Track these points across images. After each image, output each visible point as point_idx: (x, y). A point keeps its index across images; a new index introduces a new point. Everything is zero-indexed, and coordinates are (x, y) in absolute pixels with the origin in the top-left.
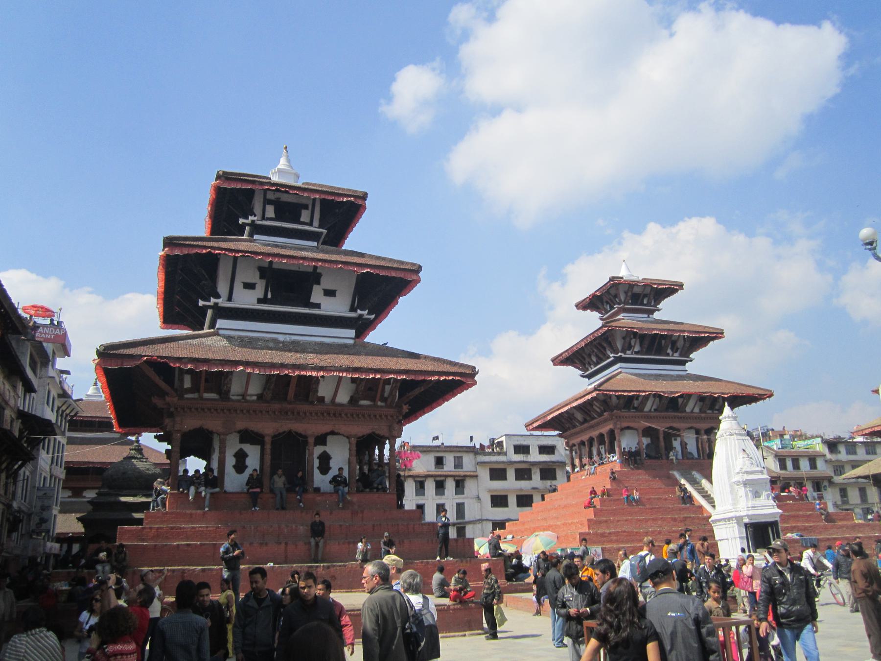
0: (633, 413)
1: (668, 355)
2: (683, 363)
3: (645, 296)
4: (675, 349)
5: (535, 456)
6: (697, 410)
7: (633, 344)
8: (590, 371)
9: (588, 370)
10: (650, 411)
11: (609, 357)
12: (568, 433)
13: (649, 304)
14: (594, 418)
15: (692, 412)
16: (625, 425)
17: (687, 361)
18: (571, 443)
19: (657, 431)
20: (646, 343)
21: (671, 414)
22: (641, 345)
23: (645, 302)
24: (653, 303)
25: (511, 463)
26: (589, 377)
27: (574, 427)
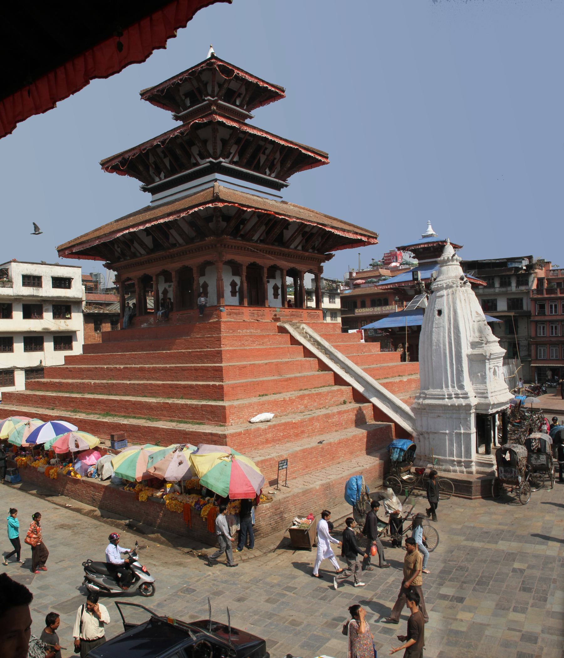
0: (239, 242)
1: (265, 174)
2: (278, 187)
3: (239, 95)
4: (271, 171)
5: (47, 290)
6: (300, 248)
7: (233, 151)
8: (158, 182)
9: (153, 182)
10: (257, 242)
11: (197, 164)
12: (123, 263)
13: (241, 106)
14: (174, 245)
15: (296, 248)
16: (228, 257)
17: (283, 186)
18: (124, 277)
19: (260, 268)
20: (250, 151)
21: (276, 248)
22: (241, 155)
23: (238, 103)
24: (245, 108)
25: (18, 299)
26: (154, 191)
27: (134, 256)
